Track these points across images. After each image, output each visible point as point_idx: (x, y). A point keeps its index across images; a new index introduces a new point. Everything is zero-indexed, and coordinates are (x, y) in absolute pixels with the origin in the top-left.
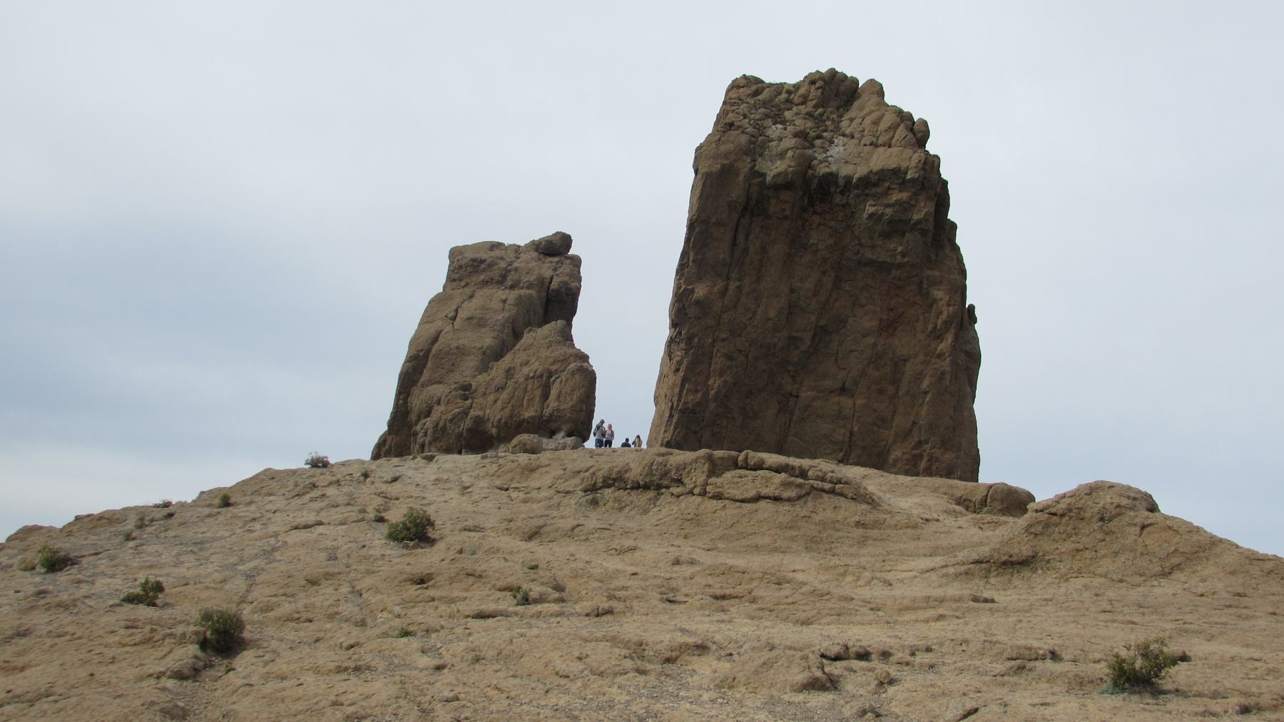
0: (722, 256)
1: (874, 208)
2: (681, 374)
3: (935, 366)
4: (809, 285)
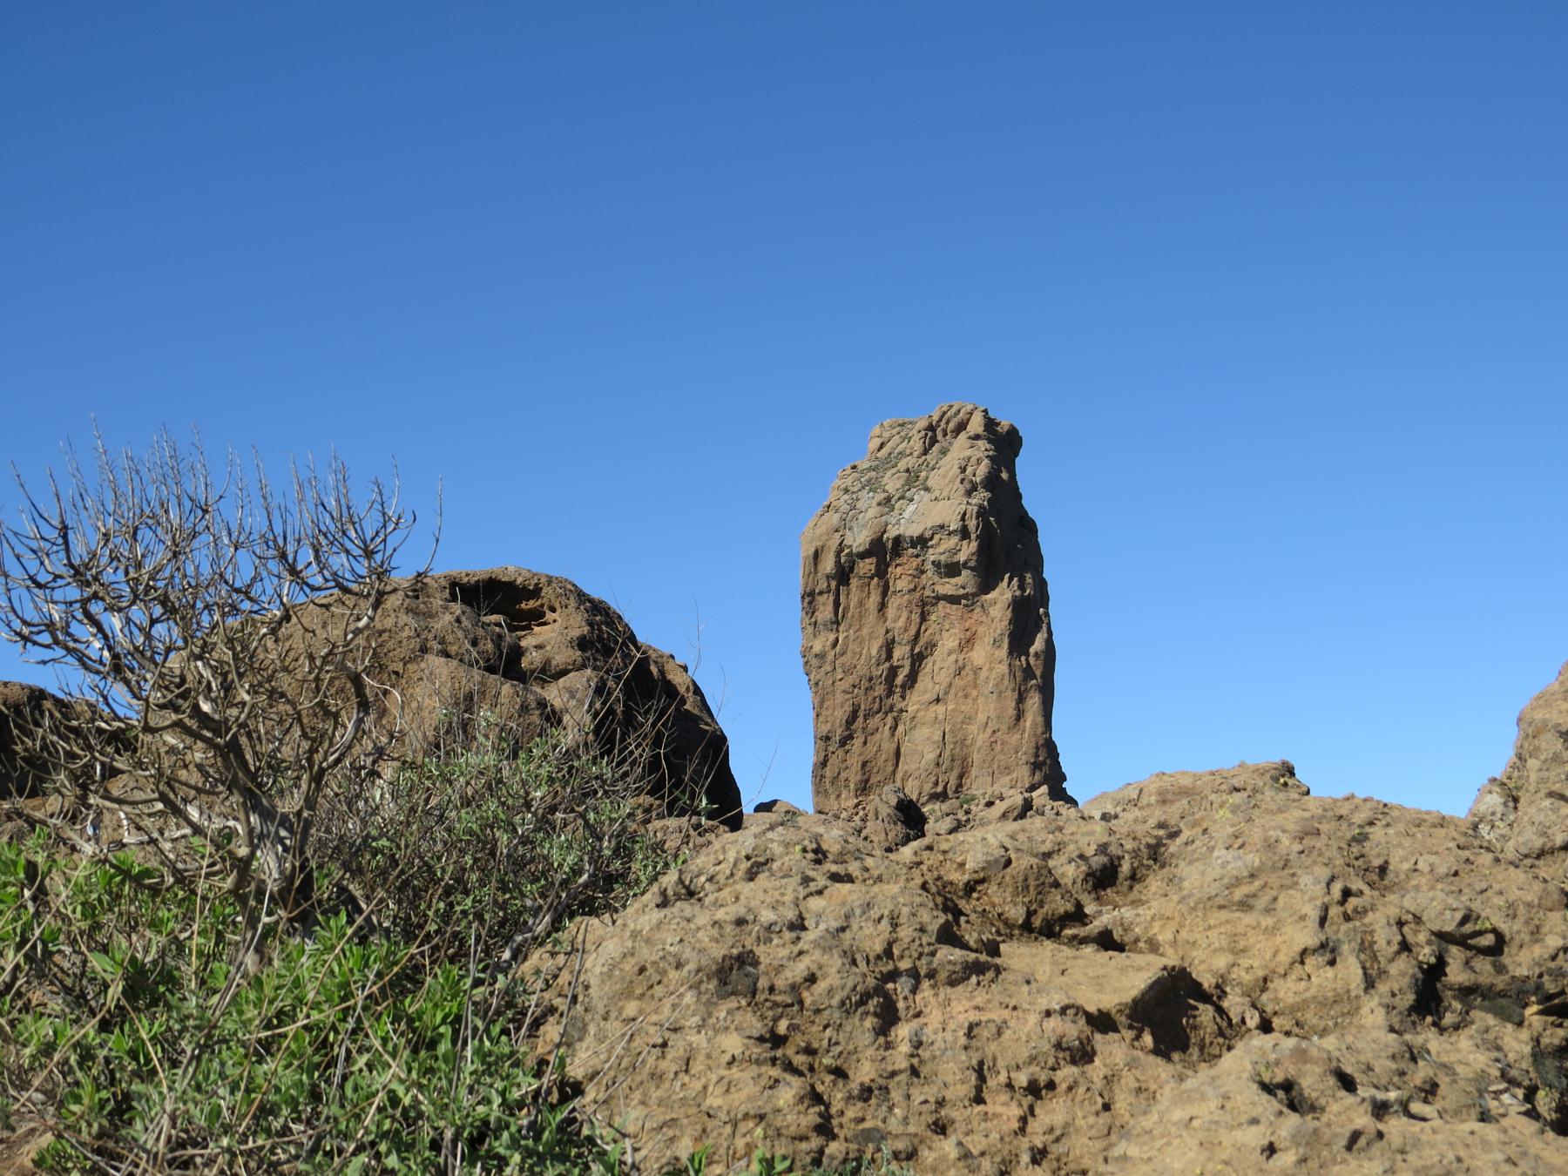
4: (901, 623)
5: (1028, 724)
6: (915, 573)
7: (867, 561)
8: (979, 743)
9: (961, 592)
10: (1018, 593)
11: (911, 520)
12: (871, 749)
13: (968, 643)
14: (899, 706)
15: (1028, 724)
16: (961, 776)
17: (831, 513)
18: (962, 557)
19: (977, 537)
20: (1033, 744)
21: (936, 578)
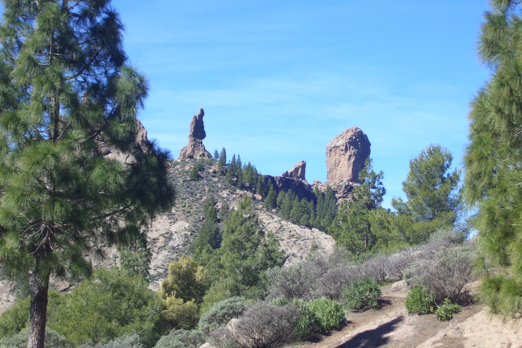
13: (344, 160)
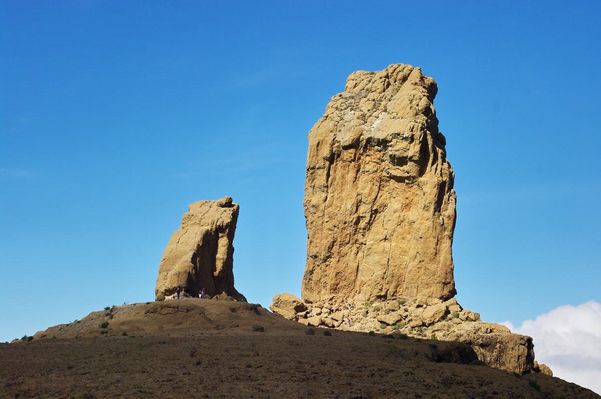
0: (323, 183)
1: (391, 152)
2: (309, 240)
3: (426, 225)
4: (366, 191)
5: (442, 258)
6: (378, 161)
7: (350, 151)
8: (410, 267)
9: (406, 175)
10: (440, 179)
11: (378, 129)
12: (341, 266)
14: (361, 240)
15: (442, 258)
16: (397, 287)
17: (328, 121)
18: (410, 154)
19: (420, 142)
20: (444, 272)
21: (391, 166)
